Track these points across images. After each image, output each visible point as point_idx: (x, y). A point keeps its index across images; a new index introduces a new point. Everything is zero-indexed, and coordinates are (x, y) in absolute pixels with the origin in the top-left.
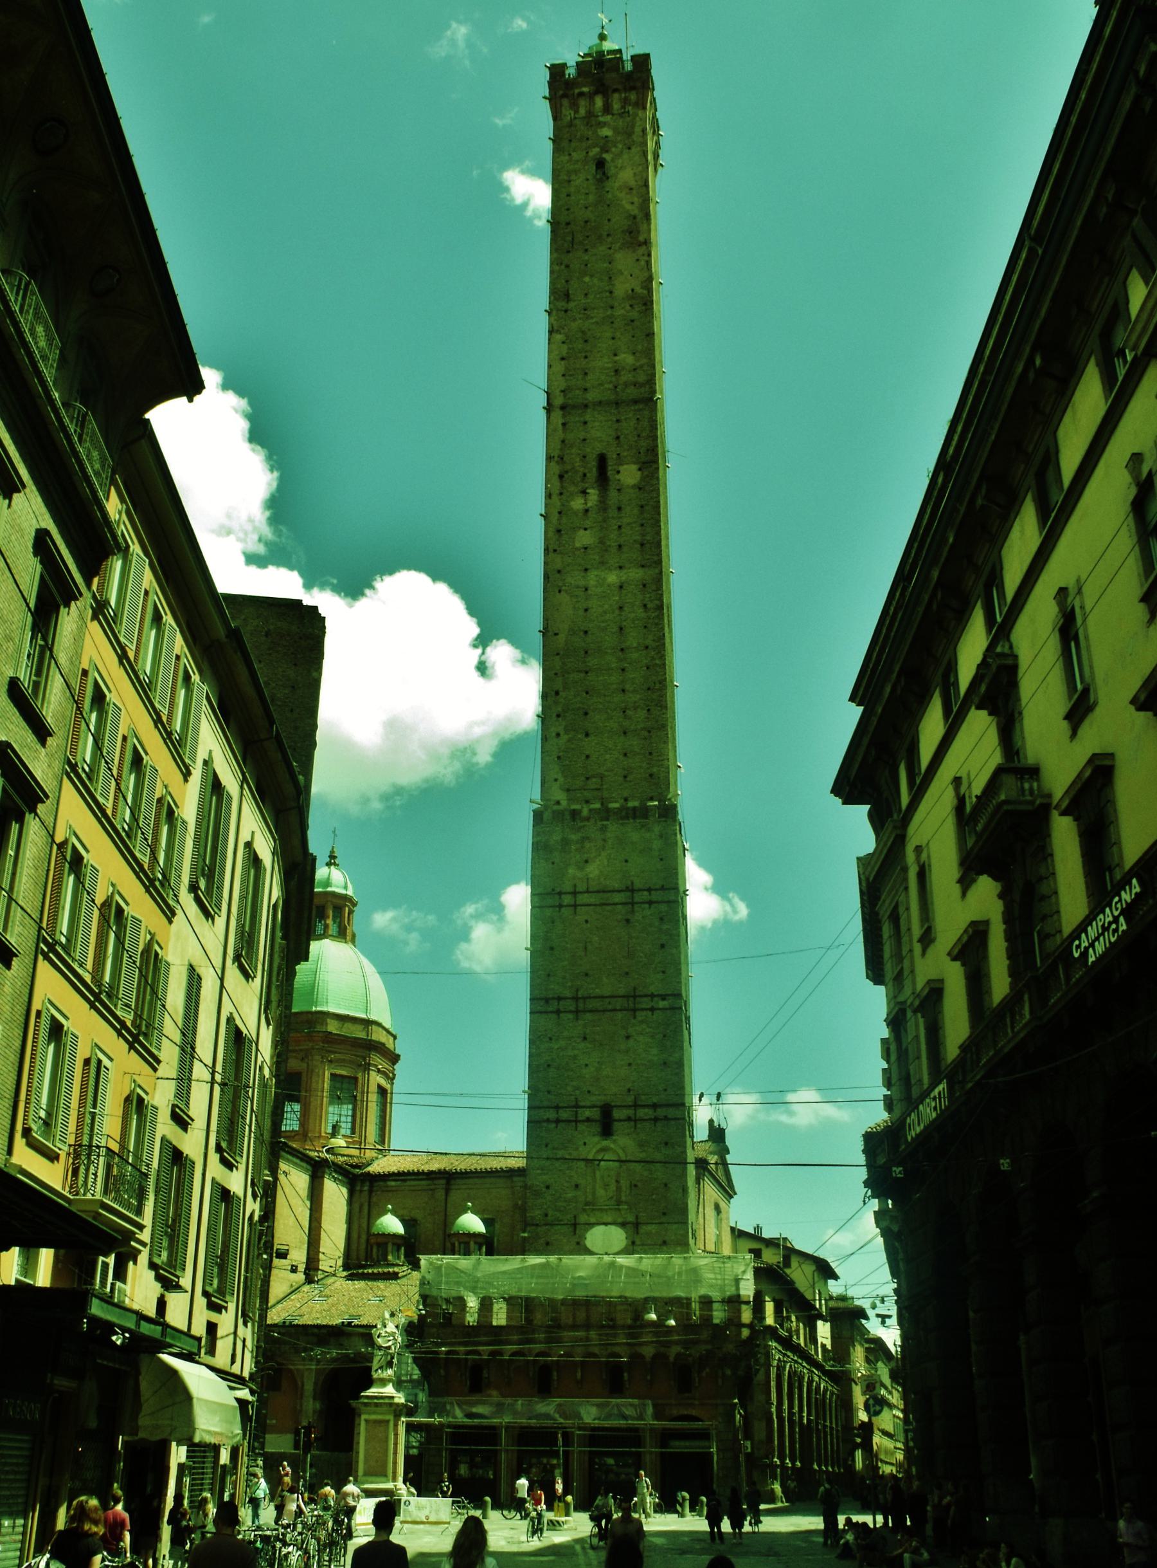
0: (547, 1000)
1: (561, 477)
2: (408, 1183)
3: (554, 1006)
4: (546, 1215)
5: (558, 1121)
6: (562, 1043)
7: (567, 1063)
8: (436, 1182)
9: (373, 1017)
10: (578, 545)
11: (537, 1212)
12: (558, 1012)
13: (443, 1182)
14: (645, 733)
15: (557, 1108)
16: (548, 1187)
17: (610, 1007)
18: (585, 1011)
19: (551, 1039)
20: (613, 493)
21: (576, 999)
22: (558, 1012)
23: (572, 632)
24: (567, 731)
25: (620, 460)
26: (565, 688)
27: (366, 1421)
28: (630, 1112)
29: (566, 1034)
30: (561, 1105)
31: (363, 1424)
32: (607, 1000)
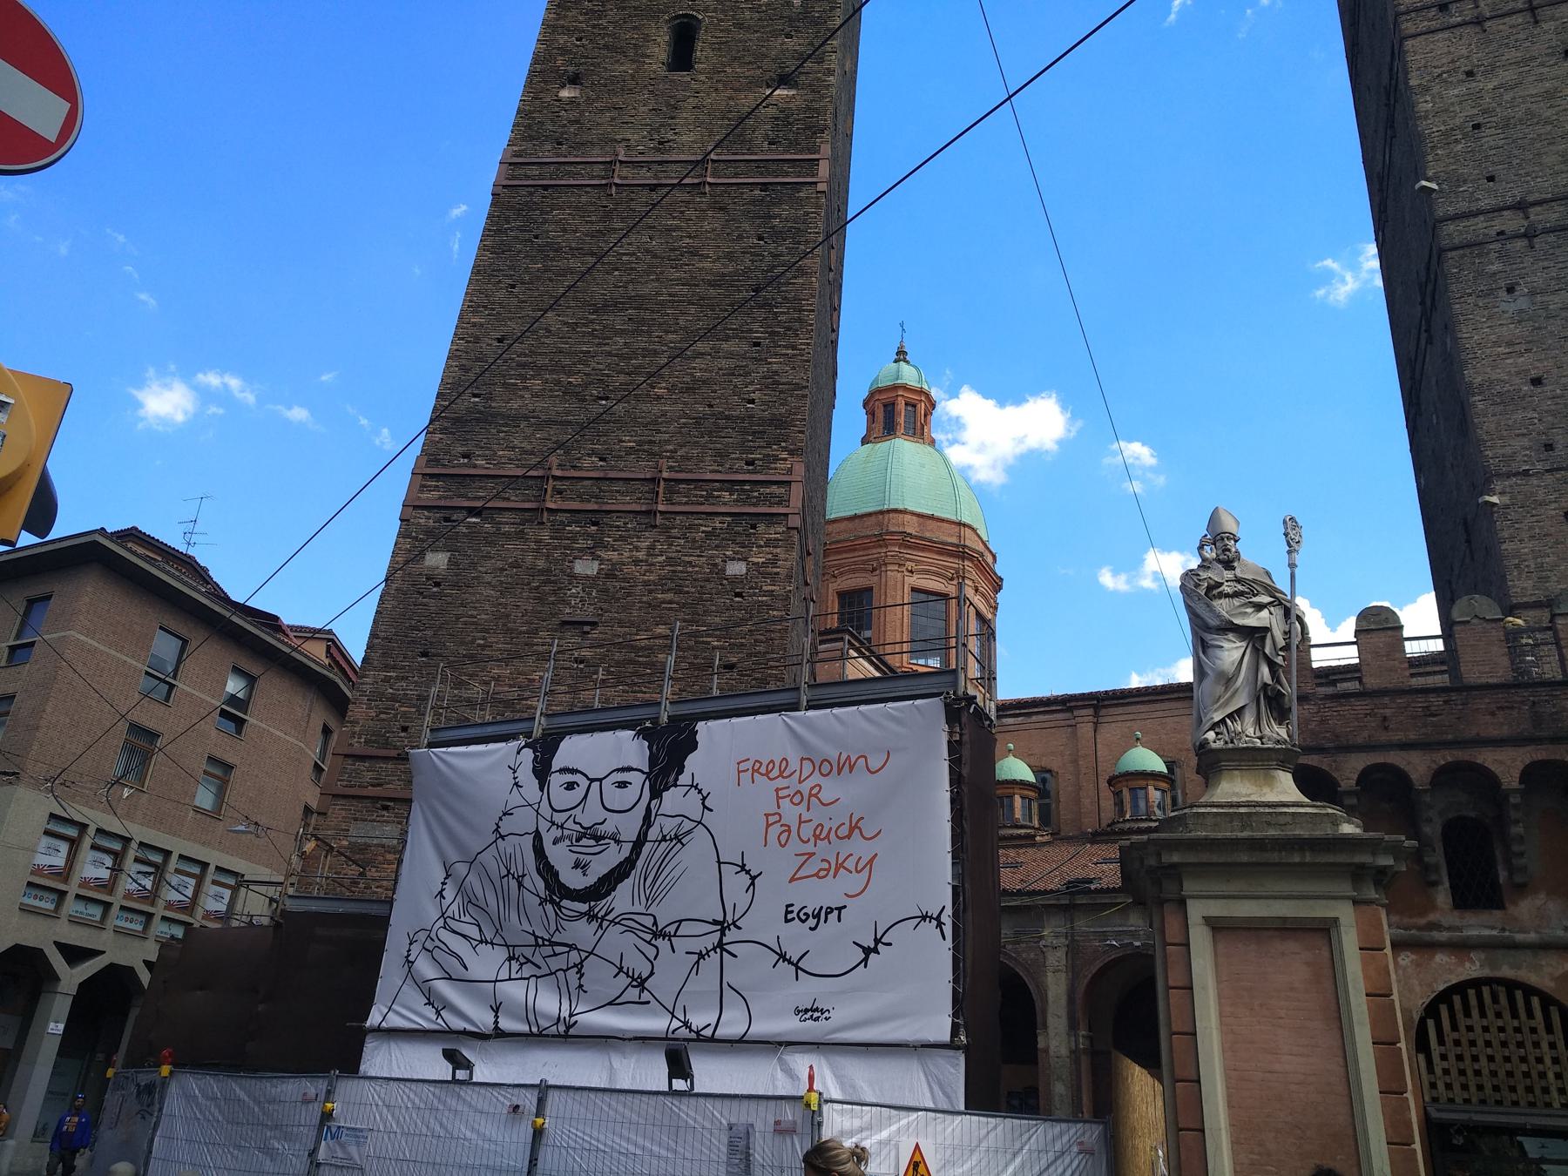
2: (1034, 718)
4: (1549, 447)
5: (1529, 235)
6: (1507, 75)
7: (1529, 112)
8: (1076, 713)
9: (965, 520)
11: (1517, 443)
12: (1478, 21)
13: (1090, 711)
15: (1521, 206)
16: (1537, 382)
19: (1470, 74)
22: (1478, 21)
27: (1208, 921)
29: (1512, 55)
30: (1531, 199)
31: (1200, 939)
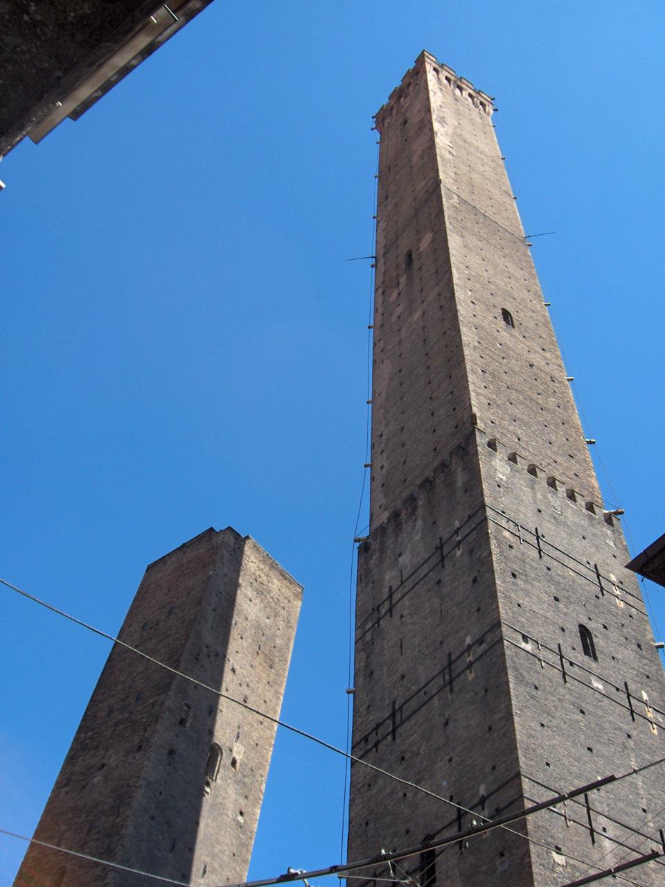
0: (366, 739)
1: (383, 293)
3: (373, 739)
10: (394, 320)
12: (376, 745)
14: (450, 396)
17: (426, 698)
18: (402, 723)
20: (416, 265)
21: (393, 715)
23: (392, 379)
24: (388, 458)
25: (419, 240)
26: (387, 425)
28: (453, 831)
32: (422, 692)
